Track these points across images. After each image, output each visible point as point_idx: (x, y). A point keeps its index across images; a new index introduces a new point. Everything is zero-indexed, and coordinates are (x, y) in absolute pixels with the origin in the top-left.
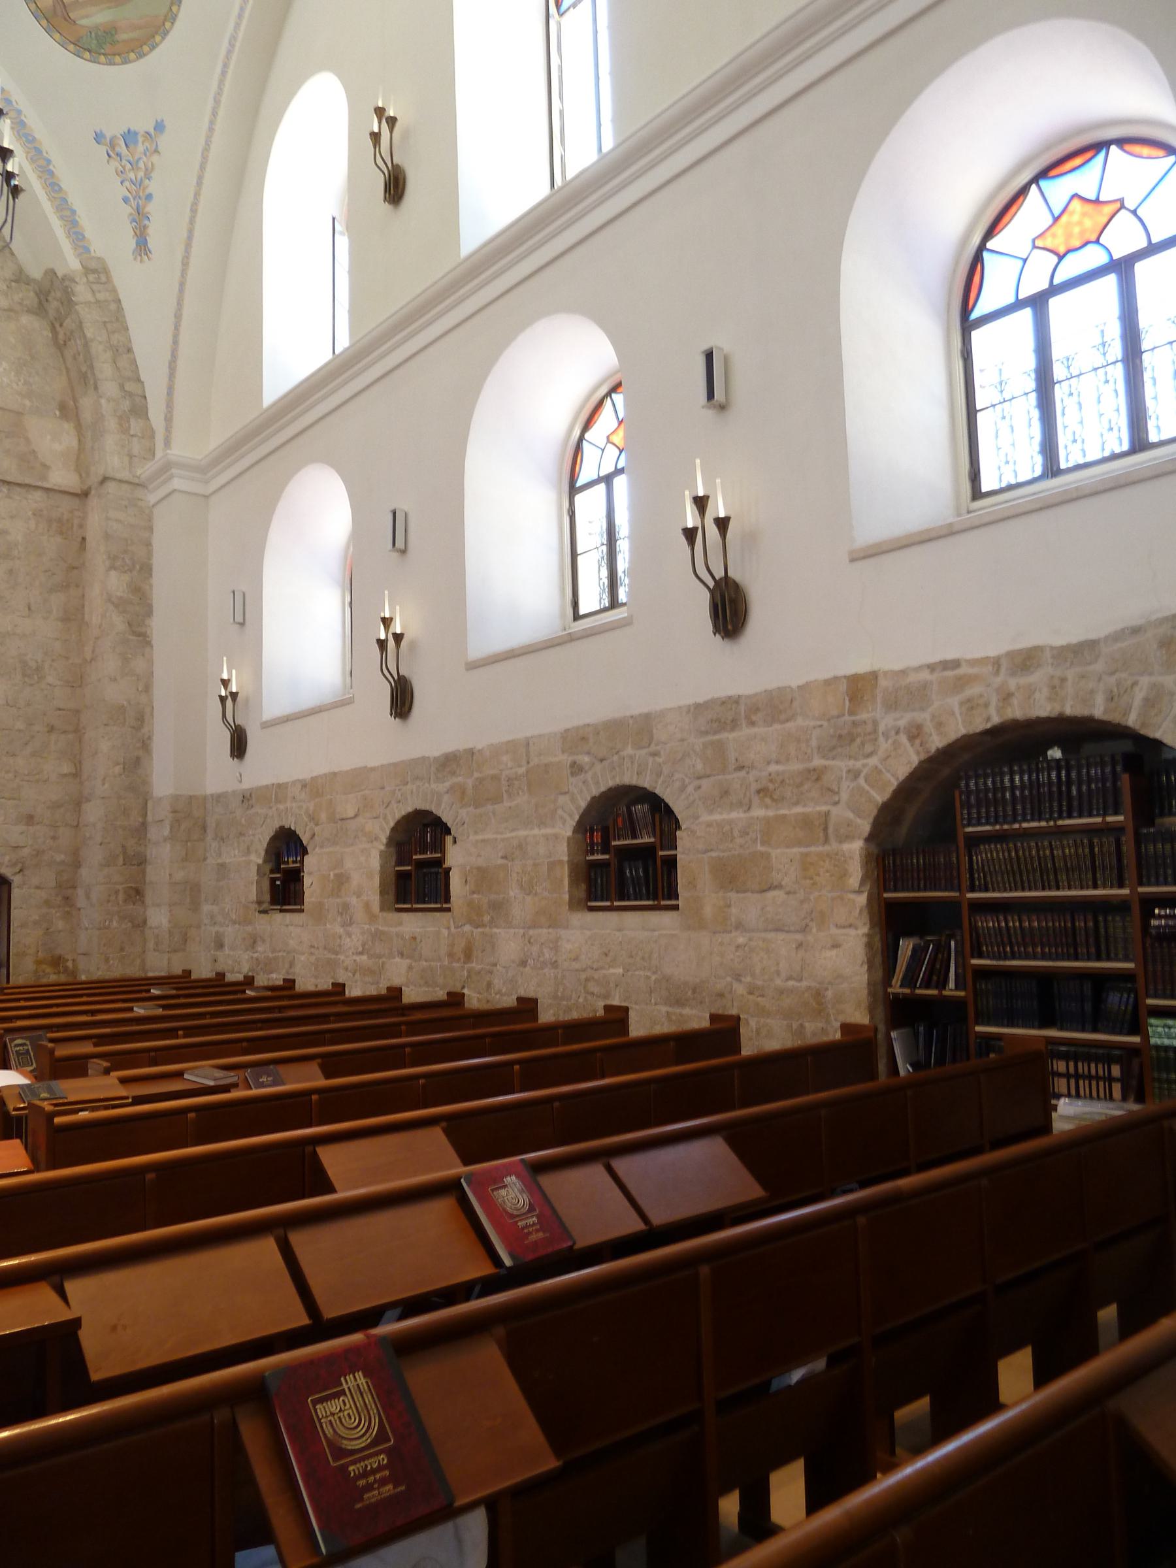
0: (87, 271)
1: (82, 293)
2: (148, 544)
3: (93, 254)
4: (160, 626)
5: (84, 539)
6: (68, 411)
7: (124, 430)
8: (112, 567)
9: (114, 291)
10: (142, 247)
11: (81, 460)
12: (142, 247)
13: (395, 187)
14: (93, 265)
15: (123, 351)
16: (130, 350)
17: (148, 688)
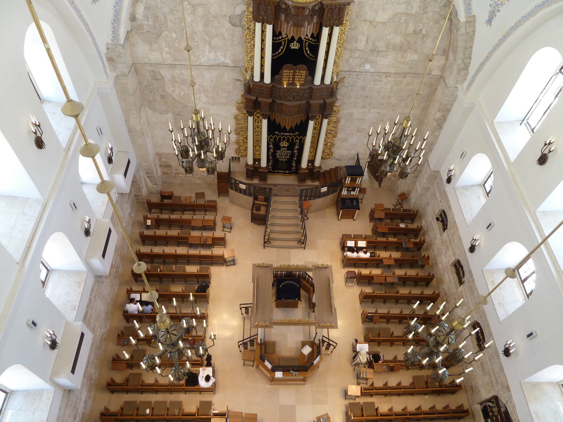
0: (467, 22)
1: (462, 31)
2: (452, 105)
3: (472, 14)
4: (446, 125)
5: (436, 89)
6: (445, 53)
7: (459, 73)
8: (439, 111)
9: (475, 28)
10: (489, 21)
11: (443, 69)
12: (489, 21)
13: (543, 160)
14: (470, 19)
15: (469, 48)
16: (471, 48)
17: (437, 138)
